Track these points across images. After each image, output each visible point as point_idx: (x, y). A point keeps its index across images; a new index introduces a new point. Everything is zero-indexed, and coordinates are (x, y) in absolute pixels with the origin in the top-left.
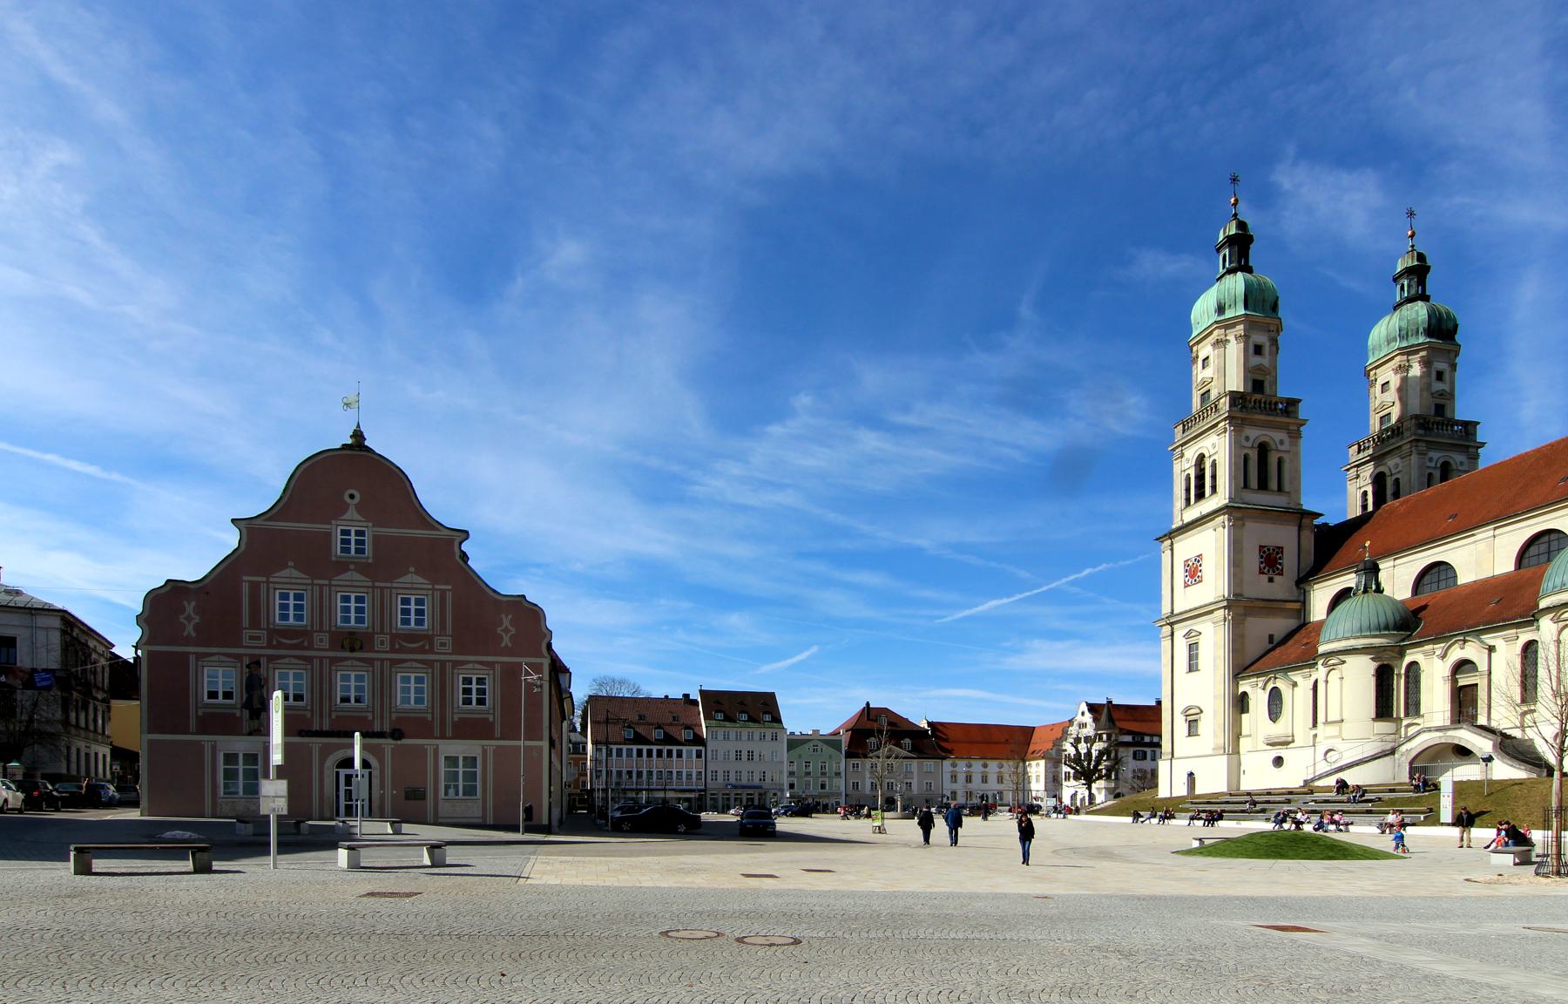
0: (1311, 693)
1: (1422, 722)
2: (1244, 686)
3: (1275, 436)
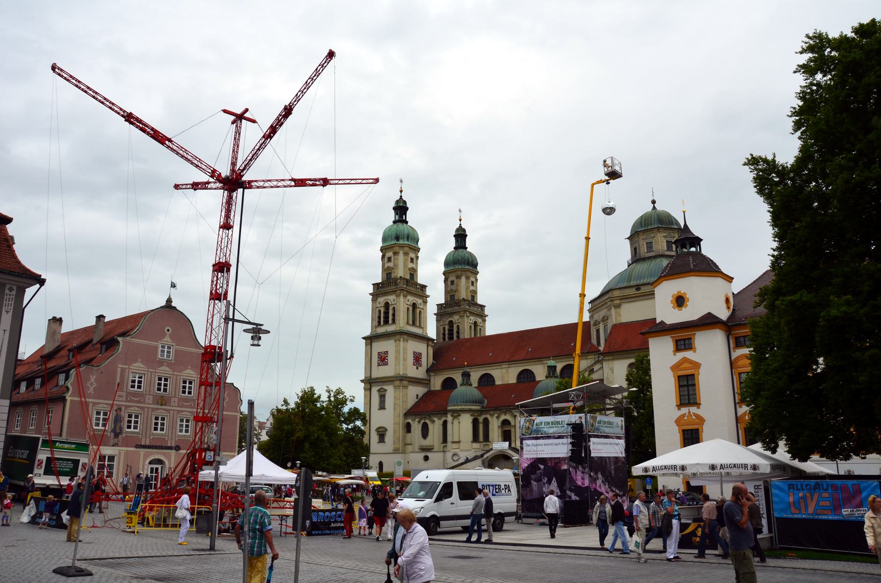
0: (441, 427)
2: (410, 421)
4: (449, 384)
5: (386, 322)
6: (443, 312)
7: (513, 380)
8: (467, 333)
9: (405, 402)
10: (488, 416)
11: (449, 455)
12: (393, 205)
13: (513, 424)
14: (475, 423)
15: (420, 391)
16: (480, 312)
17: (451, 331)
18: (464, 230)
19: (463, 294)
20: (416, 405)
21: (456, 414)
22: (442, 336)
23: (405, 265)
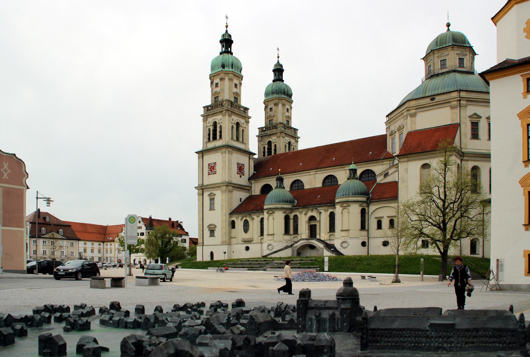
0: (259, 223)
1: (299, 237)
3: (242, 121)
4: (267, 189)
5: (215, 138)
6: (263, 133)
7: (319, 185)
8: (281, 149)
9: (230, 204)
10: (298, 214)
11: (265, 245)
12: (220, 38)
13: (318, 219)
14: (287, 218)
15: (244, 195)
16: (293, 134)
17: (270, 149)
18: (281, 66)
19: (280, 119)
20: (240, 205)
21: (272, 211)
22: (262, 154)
23: (230, 89)
